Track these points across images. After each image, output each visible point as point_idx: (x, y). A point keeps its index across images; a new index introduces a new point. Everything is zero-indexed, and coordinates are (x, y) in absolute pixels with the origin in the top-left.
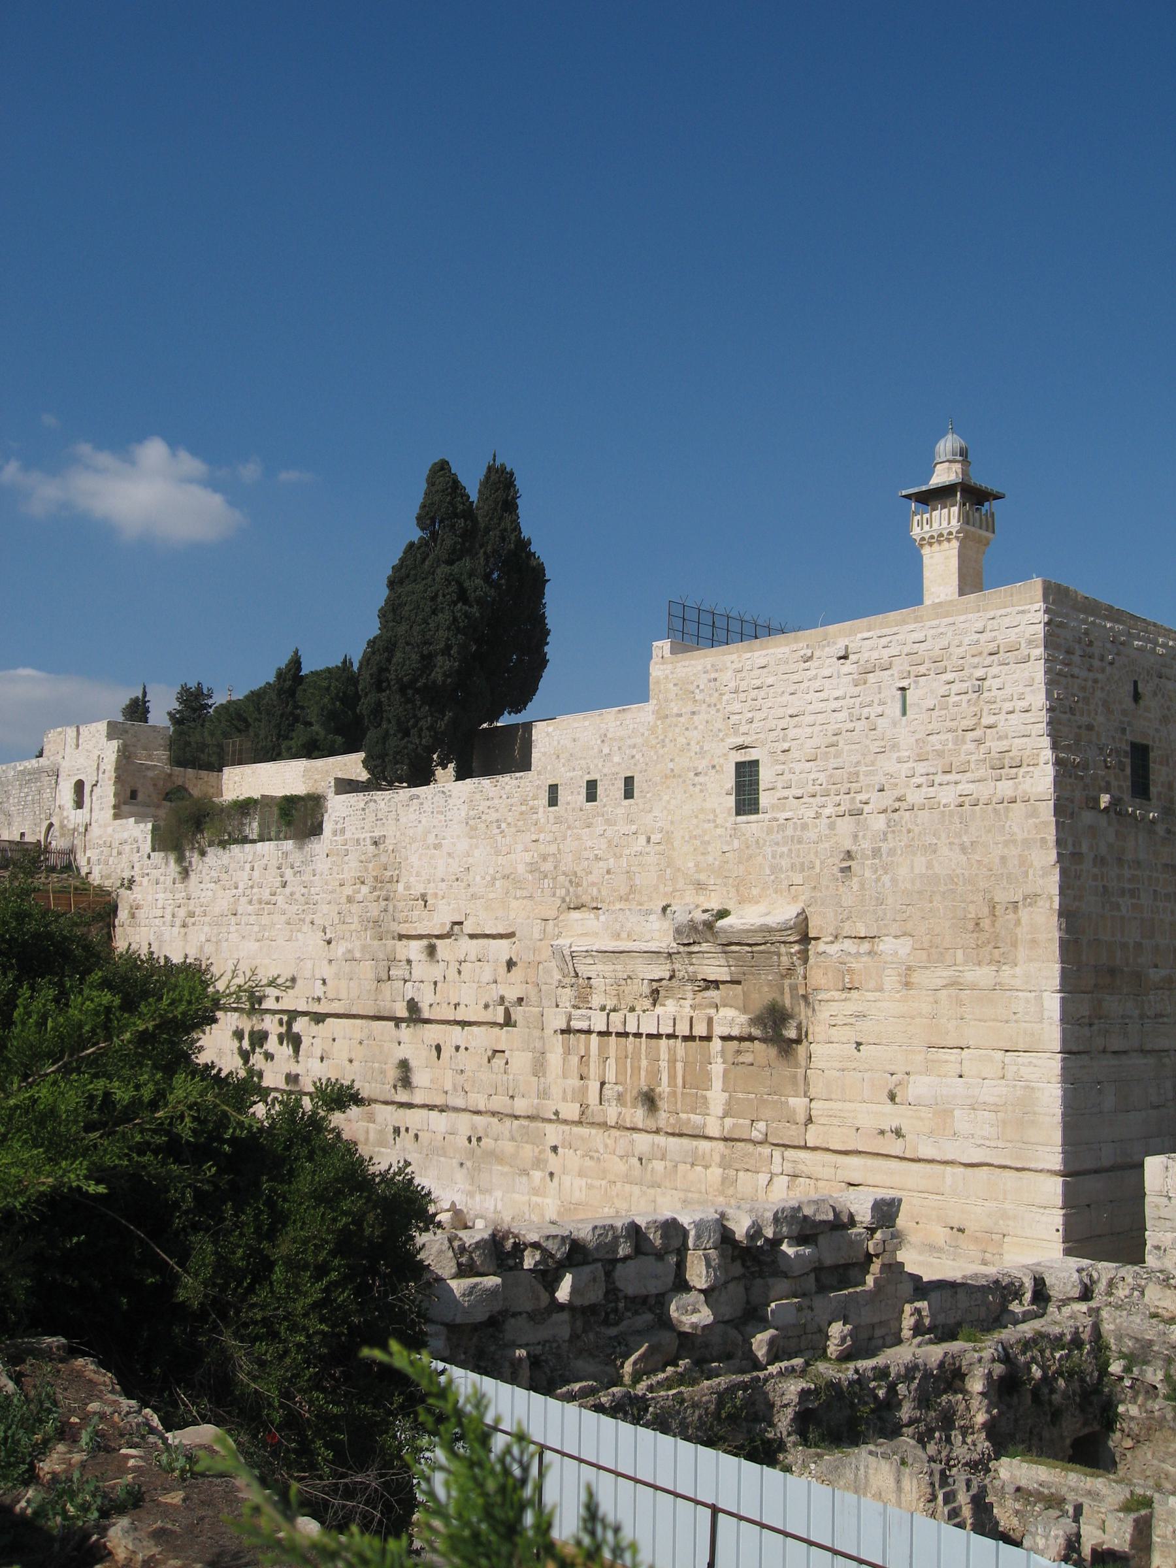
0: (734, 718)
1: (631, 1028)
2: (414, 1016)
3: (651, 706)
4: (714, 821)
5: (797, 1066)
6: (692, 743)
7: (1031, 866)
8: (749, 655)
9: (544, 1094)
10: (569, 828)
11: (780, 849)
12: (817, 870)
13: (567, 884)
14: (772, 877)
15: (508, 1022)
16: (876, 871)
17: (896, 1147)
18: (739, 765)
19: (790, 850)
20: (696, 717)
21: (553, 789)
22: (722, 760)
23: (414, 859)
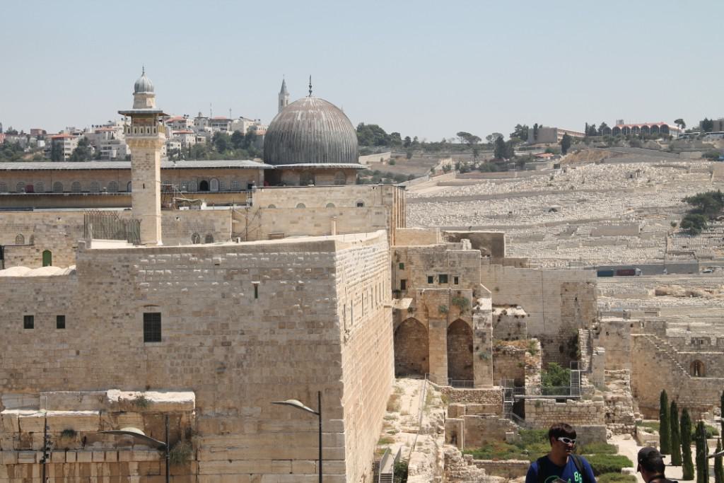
0: (142, 291)
4: (129, 344)
5: (189, 472)
7: (329, 374)
8: (152, 256)
10: (9, 342)
11: (175, 361)
12: (202, 372)
13: (8, 377)
14: (171, 375)
16: (239, 374)
18: (146, 315)
19: (183, 362)
20: (113, 286)
22: (134, 311)
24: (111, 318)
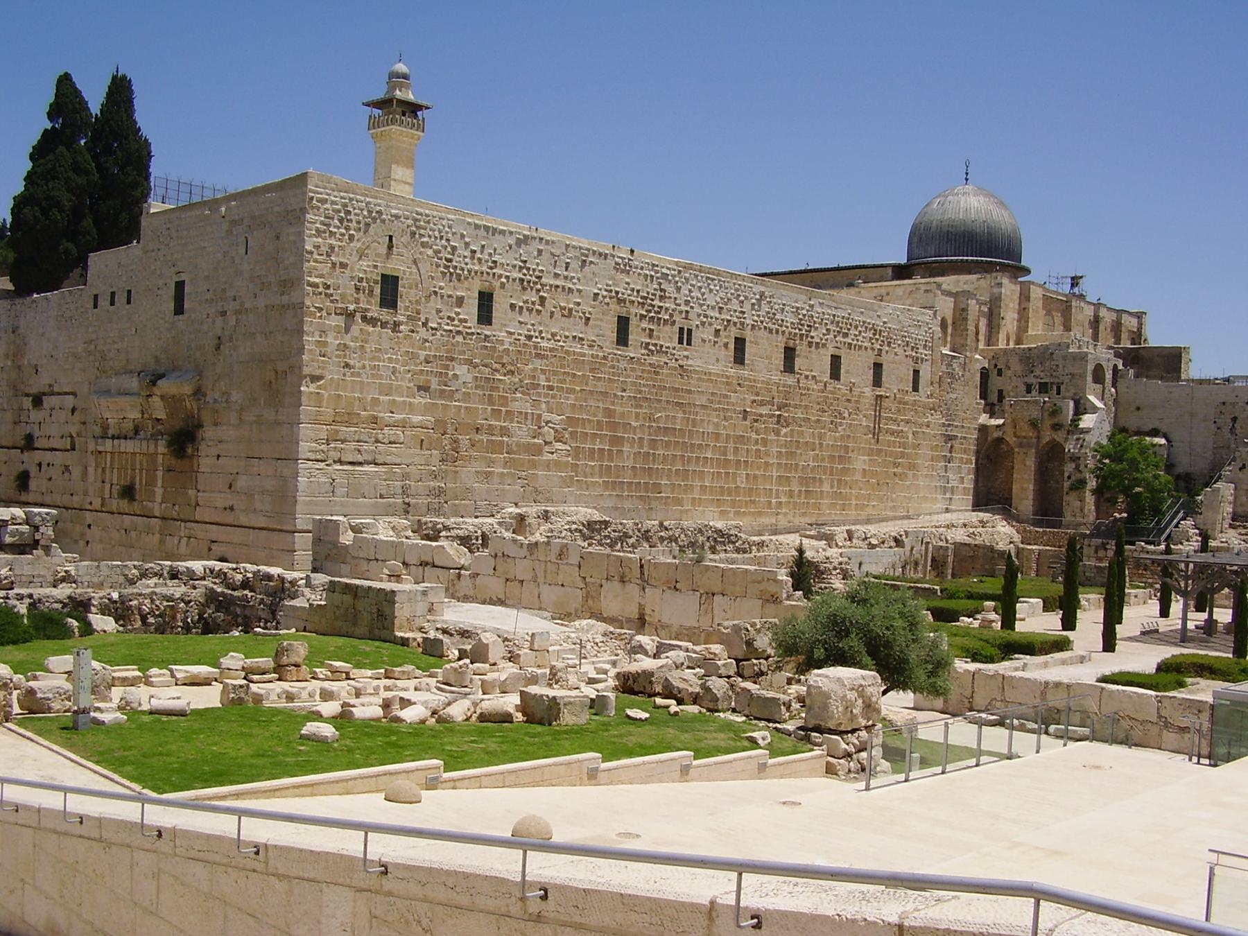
1: (122, 450)
2: (29, 443)
9: (86, 494)
15: (73, 449)
17: (229, 520)
21: (96, 296)
23: (32, 342)
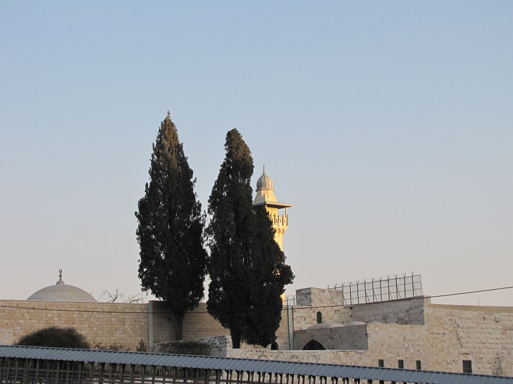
3: (426, 326)
6: (445, 348)
20: (445, 336)
24: (445, 363)
